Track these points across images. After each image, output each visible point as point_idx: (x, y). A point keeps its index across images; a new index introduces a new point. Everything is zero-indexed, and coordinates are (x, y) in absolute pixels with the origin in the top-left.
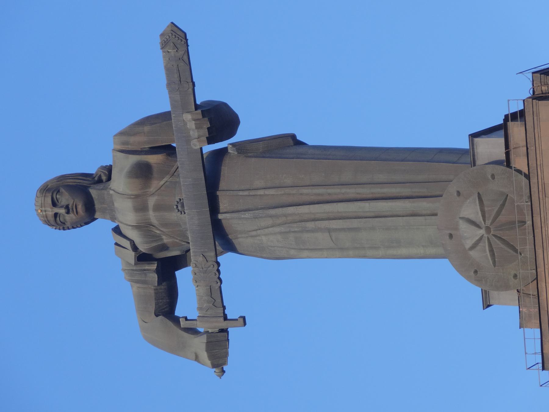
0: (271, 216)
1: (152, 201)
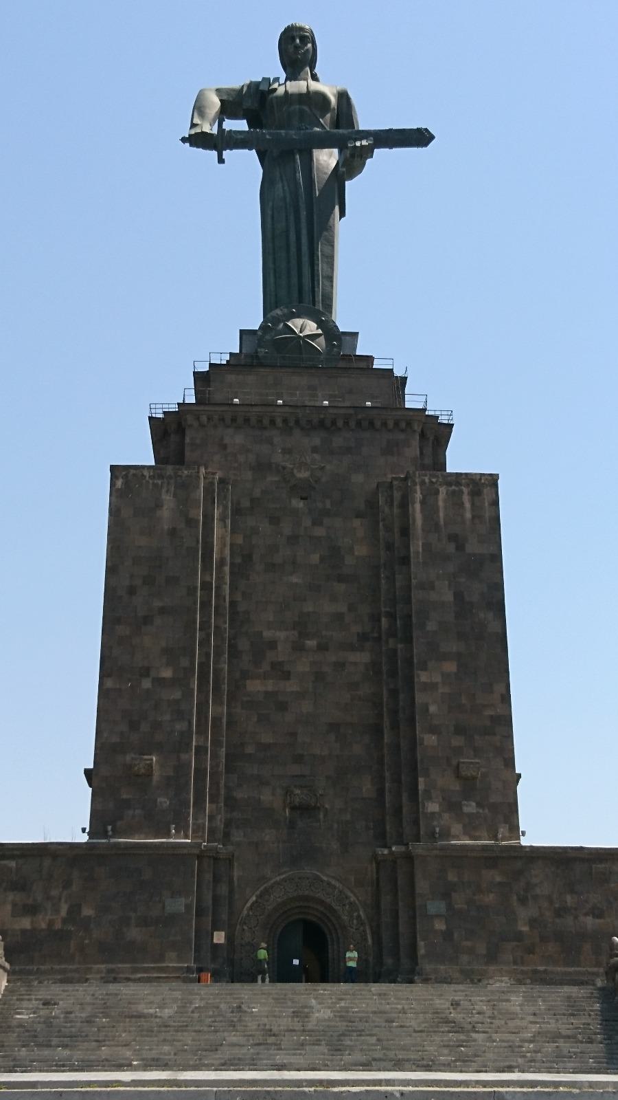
1: (306, 108)
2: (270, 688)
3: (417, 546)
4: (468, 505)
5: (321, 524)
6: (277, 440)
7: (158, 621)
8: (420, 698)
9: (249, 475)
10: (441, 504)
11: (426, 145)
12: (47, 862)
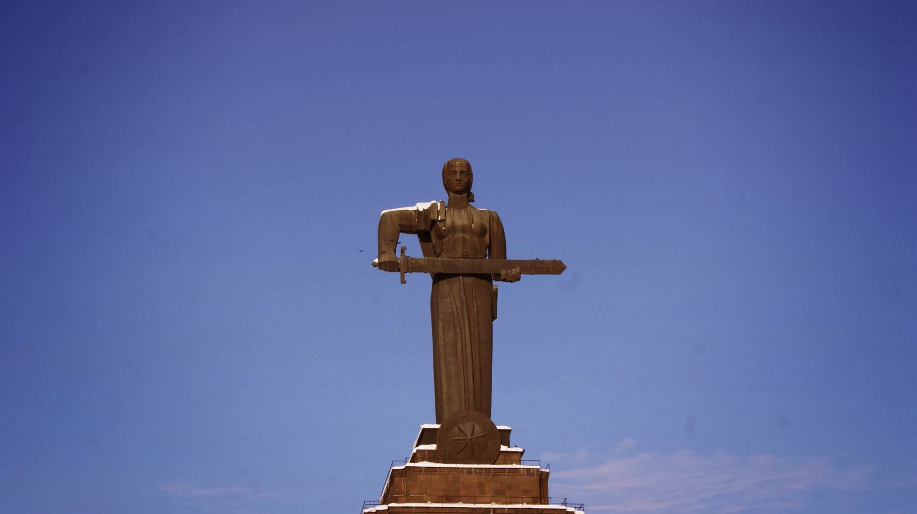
0: (462, 308)
1: (467, 236)
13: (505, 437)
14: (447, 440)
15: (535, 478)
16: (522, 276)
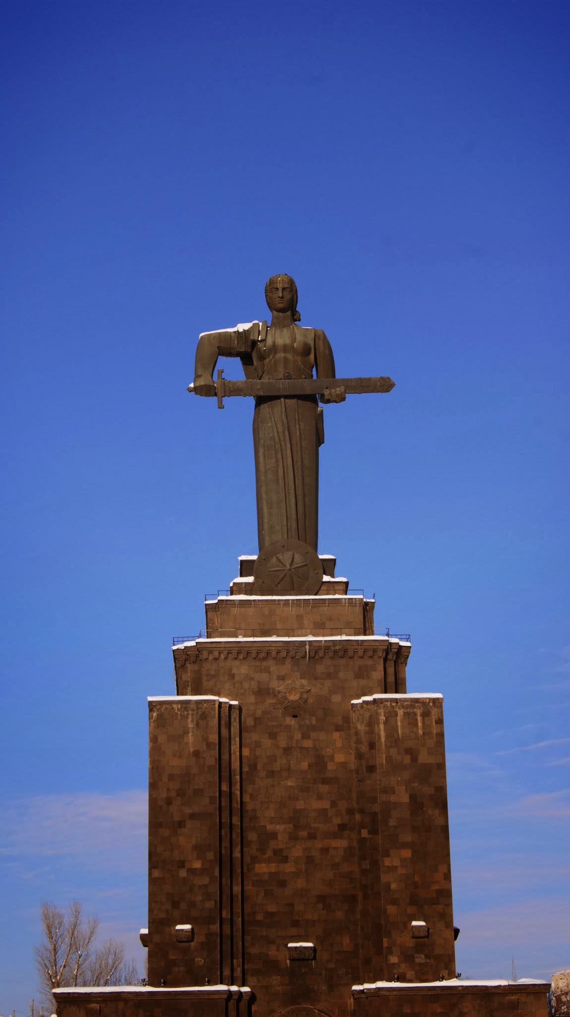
0: (284, 432)
2: (273, 870)
3: (381, 759)
4: (420, 724)
5: (309, 738)
6: (272, 669)
7: (189, 824)
8: (384, 878)
9: (252, 699)
10: (399, 724)
11: (388, 391)
12: (121, 1005)
13: (329, 567)
14: (263, 574)
15: (359, 610)
16: (347, 395)
